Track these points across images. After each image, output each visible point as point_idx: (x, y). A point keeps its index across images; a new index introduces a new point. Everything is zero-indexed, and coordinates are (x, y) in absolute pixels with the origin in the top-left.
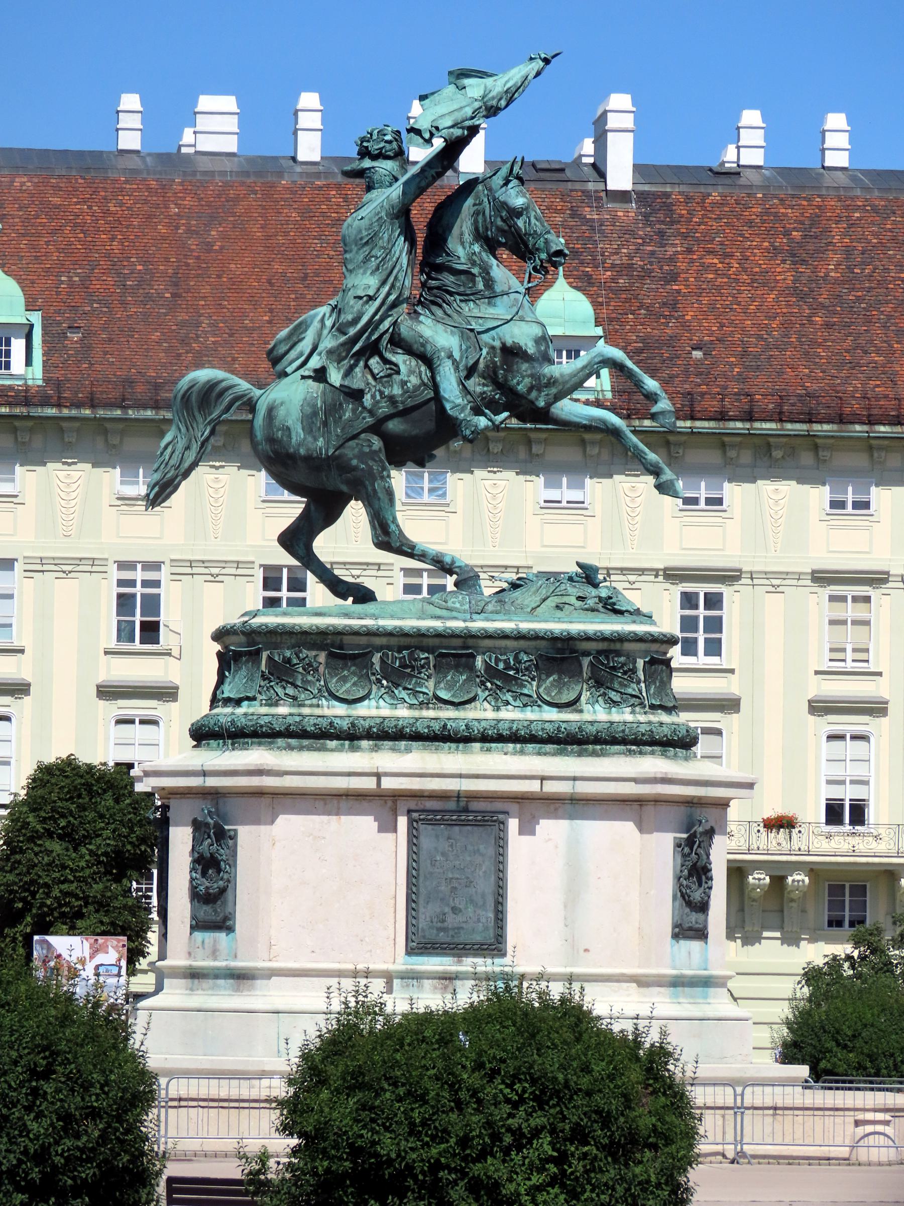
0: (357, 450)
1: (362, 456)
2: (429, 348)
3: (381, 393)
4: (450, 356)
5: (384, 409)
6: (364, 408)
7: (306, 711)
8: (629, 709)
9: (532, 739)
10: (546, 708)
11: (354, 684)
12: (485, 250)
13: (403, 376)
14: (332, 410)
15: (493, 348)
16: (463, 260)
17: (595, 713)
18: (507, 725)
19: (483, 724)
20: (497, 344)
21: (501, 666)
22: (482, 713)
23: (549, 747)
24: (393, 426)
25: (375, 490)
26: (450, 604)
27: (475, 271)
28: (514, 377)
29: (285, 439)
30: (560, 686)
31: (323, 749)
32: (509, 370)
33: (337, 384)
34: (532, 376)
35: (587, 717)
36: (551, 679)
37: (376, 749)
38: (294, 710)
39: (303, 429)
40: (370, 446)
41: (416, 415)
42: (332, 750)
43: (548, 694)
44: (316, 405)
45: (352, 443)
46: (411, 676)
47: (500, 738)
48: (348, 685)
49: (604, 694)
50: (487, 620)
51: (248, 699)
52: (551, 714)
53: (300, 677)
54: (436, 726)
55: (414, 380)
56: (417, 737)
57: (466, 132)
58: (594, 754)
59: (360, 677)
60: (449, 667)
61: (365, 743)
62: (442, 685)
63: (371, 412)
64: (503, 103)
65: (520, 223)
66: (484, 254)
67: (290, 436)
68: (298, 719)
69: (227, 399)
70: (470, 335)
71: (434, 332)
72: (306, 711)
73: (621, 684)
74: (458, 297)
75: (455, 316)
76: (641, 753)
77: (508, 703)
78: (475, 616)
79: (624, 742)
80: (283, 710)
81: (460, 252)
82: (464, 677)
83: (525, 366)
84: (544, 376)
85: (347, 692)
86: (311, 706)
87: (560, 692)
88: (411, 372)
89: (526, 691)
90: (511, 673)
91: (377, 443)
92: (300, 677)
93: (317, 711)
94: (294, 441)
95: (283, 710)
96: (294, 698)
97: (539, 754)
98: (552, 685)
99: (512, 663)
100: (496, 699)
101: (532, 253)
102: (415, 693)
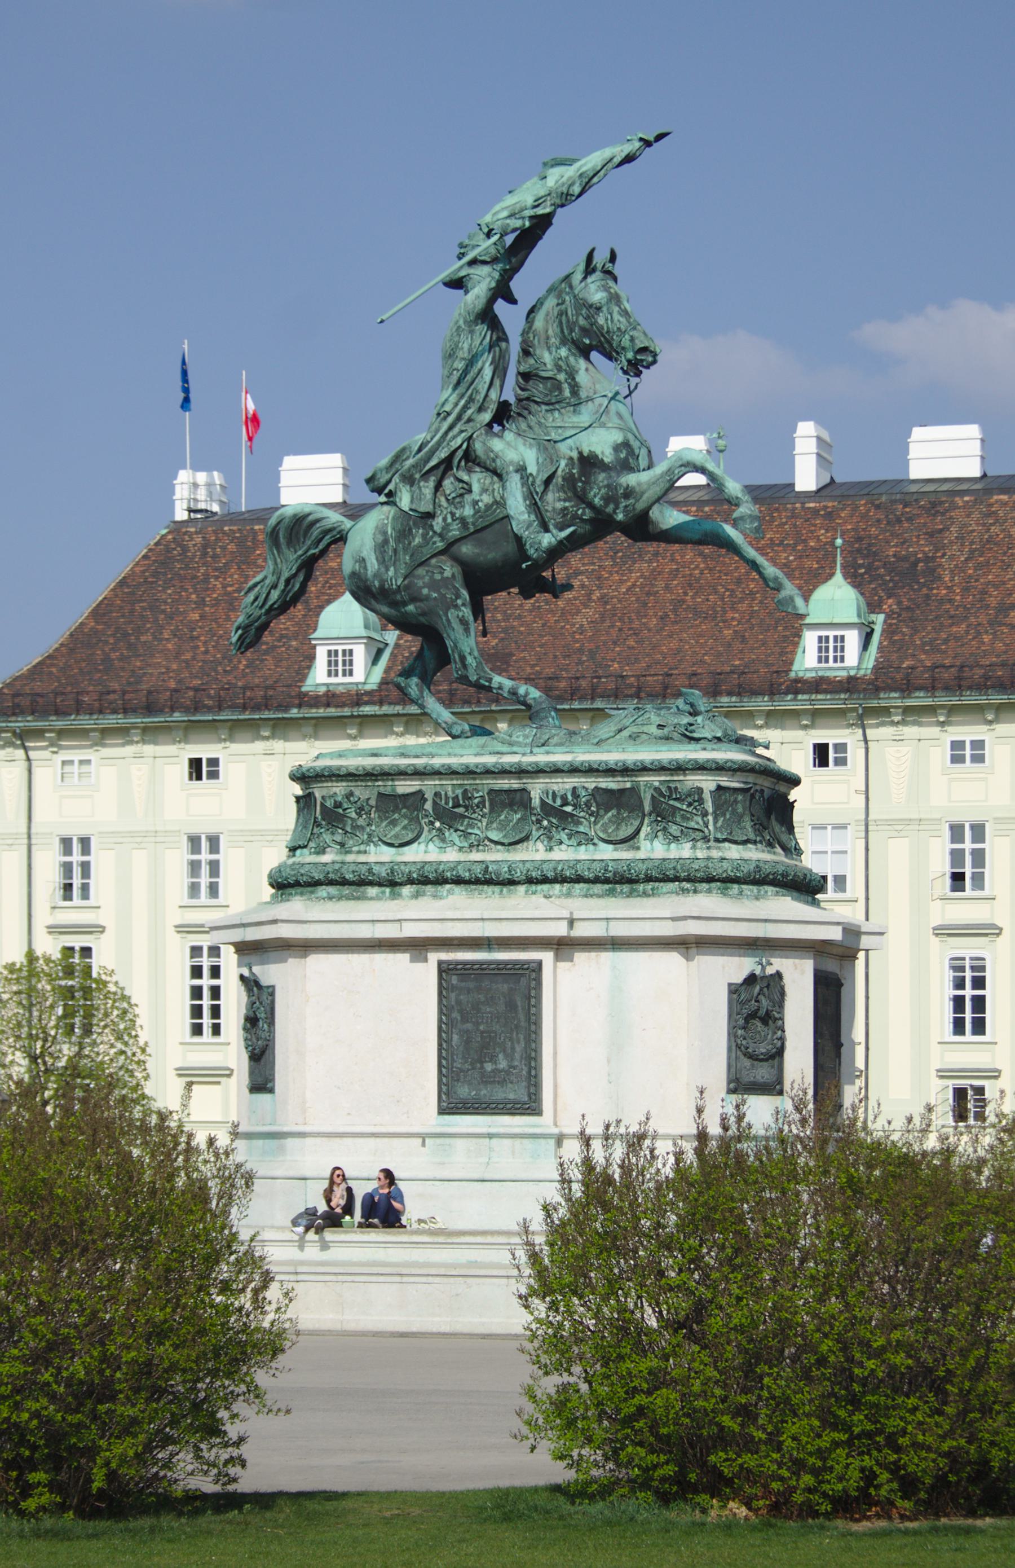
0: (427, 579)
1: (433, 585)
2: (498, 461)
3: (453, 514)
4: (521, 469)
5: (455, 532)
6: (435, 532)
7: (350, 858)
8: (689, 845)
9: (579, 879)
10: (602, 845)
11: (405, 828)
12: (574, 354)
13: (475, 495)
14: (404, 534)
15: (571, 459)
16: (549, 367)
17: (653, 849)
18: (552, 865)
19: (528, 865)
20: (575, 455)
21: (559, 802)
22: (535, 853)
23: (598, 888)
24: (466, 549)
25: (448, 620)
26: (514, 738)
27: (561, 377)
28: (591, 489)
30: (618, 821)
31: (363, 898)
32: (586, 483)
33: (406, 509)
34: (608, 486)
35: (641, 855)
37: (416, 896)
38: (339, 858)
40: (442, 573)
41: (487, 534)
42: (372, 899)
43: (605, 831)
44: (385, 533)
45: (421, 571)
46: (464, 817)
47: (545, 880)
48: (398, 829)
49: (665, 829)
50: (548, 753)
51: (300, 847)
52: (606, 852)
53: (350, 822)
54: (478, 870)
55: (487, 499)
56: (459, 881)
58: (645, 894)
59: (411, 820)
60: (504, 805)
61: (407, 890)
62: (495, 825)
63: (440, 535)
64: (576, 189)
65: (601, 320)
66: (572, 359)
68: (337, 866)
69: (315, 532)
70: (547, 447)
71: (512, 448)
72: (350, 858)
73: (684, 817)
74: (544, 407)
75: (536, 428)
76: (695, 891)
77: (561, 843)
78: (535, 750)
79: (676, 879)
80: (327, 858)
81: (547, 358)
82: (518, 816)
83: (602, 477)
84: (621, 485)
85: (396, 836)
86: (359, 852)
87: (617, 829)
88: (484, 490)
89: (581, 829)
90: (569, 809)
91: (449, 569)
92: (350, 822)
93: (362, 858)
95: (327, 858)
96: (342, 845)
97: (586, 896)
98: (610, 821)
99: (570, 797)
100: (550, 838)
101: (618, 353)
102: (466, 835)
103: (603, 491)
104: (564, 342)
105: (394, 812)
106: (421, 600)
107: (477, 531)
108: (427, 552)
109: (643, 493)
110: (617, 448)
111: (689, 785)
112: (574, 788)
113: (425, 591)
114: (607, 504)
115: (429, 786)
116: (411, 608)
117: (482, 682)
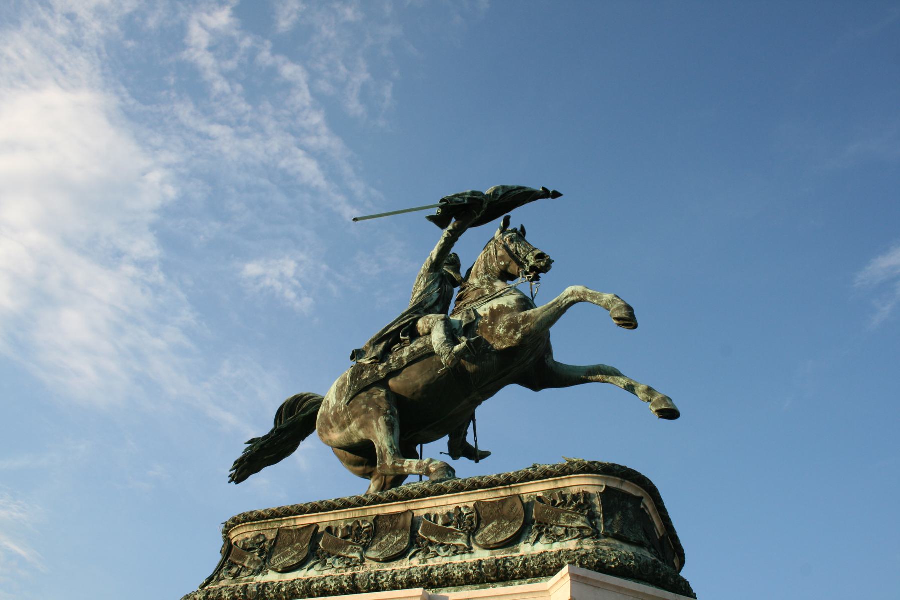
6: (379, 372)
11: (294, 558)
20: (488, 312)
34: (511, 320)
36: (491, 526)
45: (364, 394)
57: (466, 202)
62: (375, 548)
77: (438, 555)
82: (399, 538)
87: (496, 537)
89: (459, 542)
98: (489, 531)
104: (486, 273)
105: (288, 546)
108: (370, 382)
110: (518, 301)
111: (575, 491)
112: (458, 508)
114: (509, 331)
115: (324, 520)
116: (354, 426)
117: (397, 465)
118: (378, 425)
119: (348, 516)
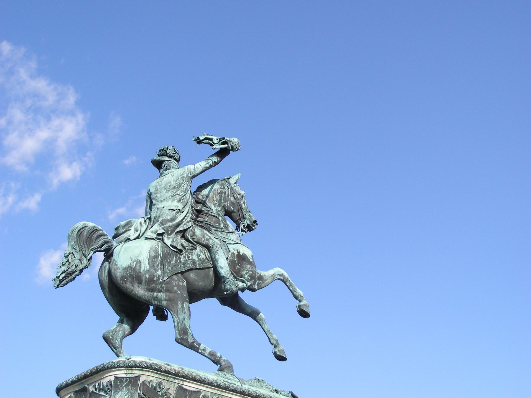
3: (189, 257)
5: (190, 265)
15: (233, 253)
20: (236, 252)
25: (183, 307)
29: (137, 267)
39: (149, 264)
44: (157, 252)
45: (175, 277)
55: (203, 256)
63: (184, 264)
67: (140, 266)
83: (249, 266)
84: (258, 273)
88: (201, 252)
91: (185, 284)
94: (143, 269)
103: (250, 273)
104: (219, 205)
106: (171, 292)
107: (199, 269)
109: (266, 280)
113: (175, 288)
117: (195, 344)
118: (183, 307)
119: (213, 391)
